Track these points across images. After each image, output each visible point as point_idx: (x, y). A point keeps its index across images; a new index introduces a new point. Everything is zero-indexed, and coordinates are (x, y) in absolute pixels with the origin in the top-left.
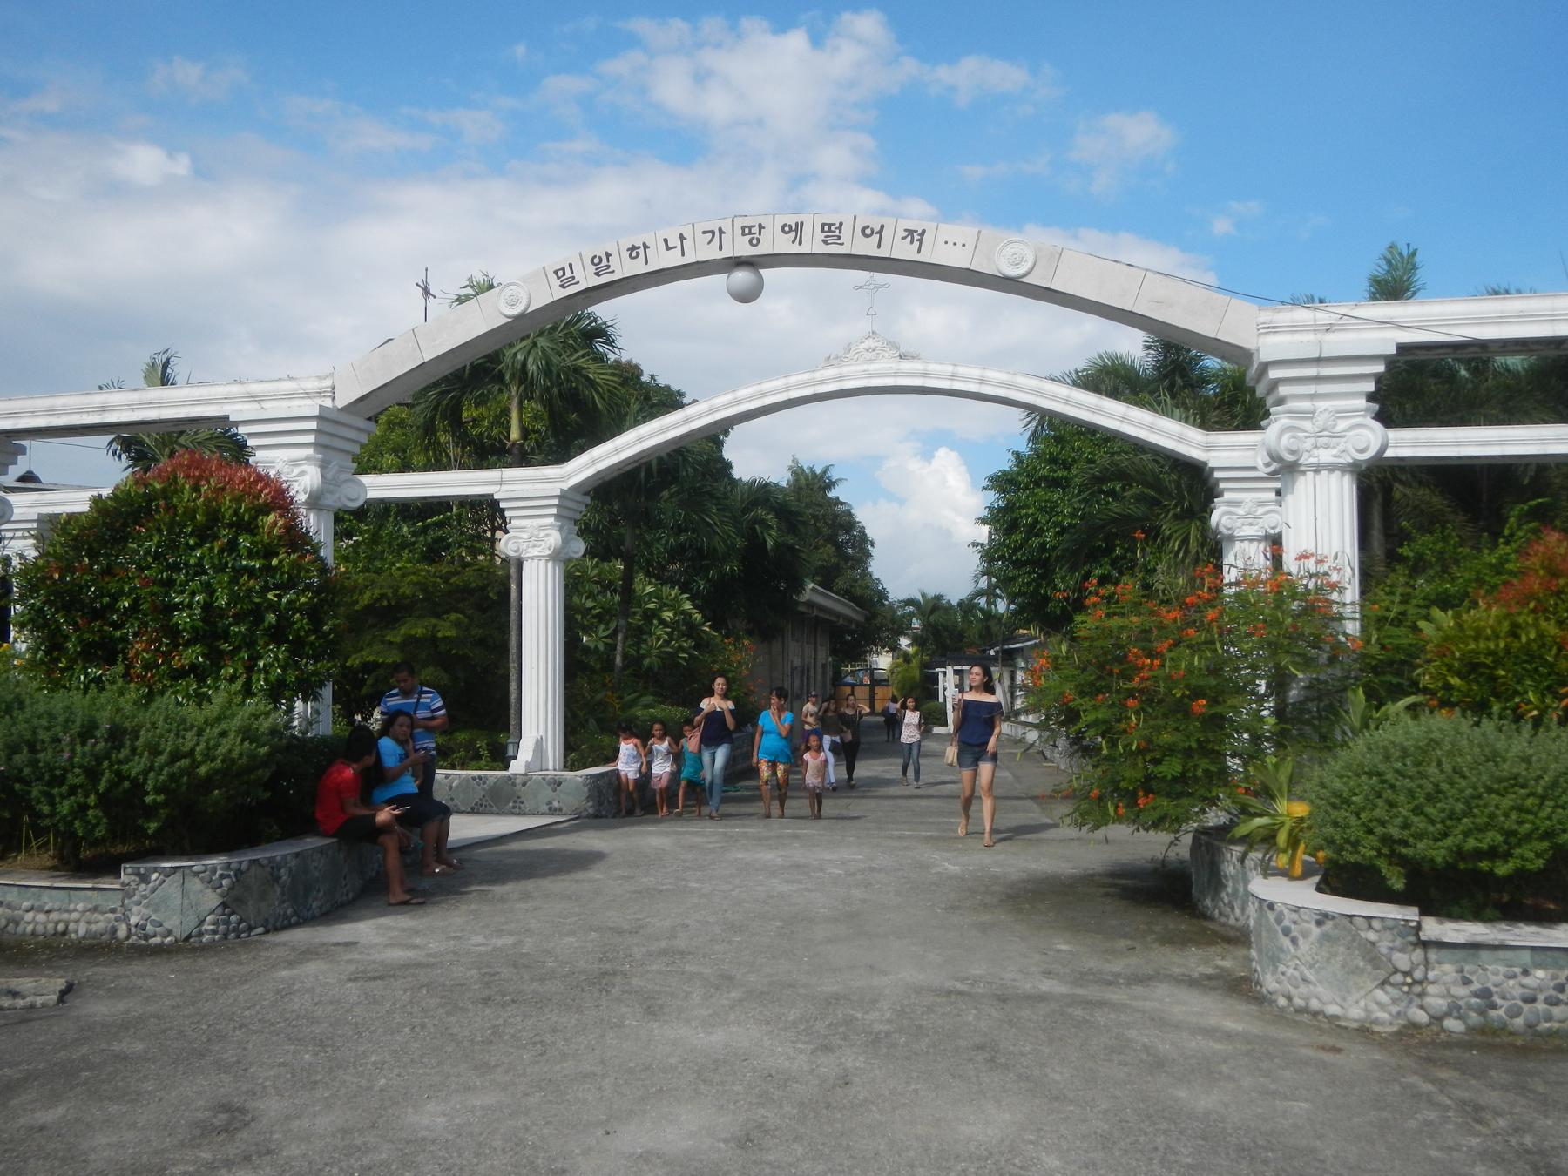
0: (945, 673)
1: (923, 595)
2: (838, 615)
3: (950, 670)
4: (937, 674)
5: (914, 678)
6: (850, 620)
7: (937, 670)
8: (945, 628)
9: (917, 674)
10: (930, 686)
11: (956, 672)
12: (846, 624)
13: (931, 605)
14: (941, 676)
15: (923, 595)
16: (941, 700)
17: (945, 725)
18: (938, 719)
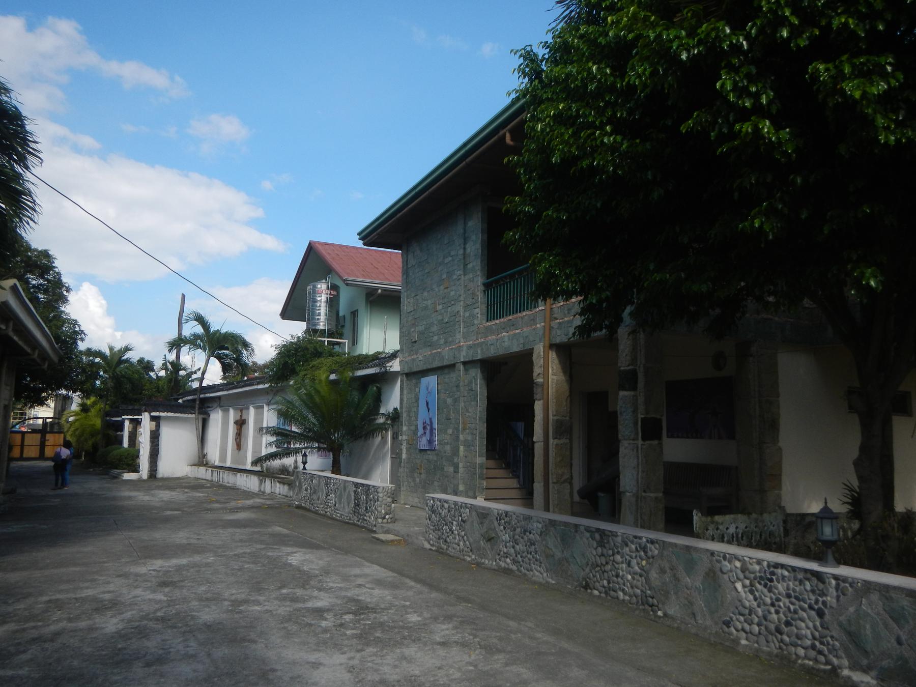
0: (136, 423)
1: (111, 349)
2: (34, 344)
3: (145, 417)
4: (123, 421)
5: (94, 425)
6: (44, 356)
7: (123, 417)
8: (130, 380)
9: (98, 423)
10: (111, 433)
11: (153, 418)
12: (38, 360)
13: (116, 359)
14: (127, 423)
15: (111, 349)
16: (126, 444)
17: (135, 469)
18: (129, 465)
